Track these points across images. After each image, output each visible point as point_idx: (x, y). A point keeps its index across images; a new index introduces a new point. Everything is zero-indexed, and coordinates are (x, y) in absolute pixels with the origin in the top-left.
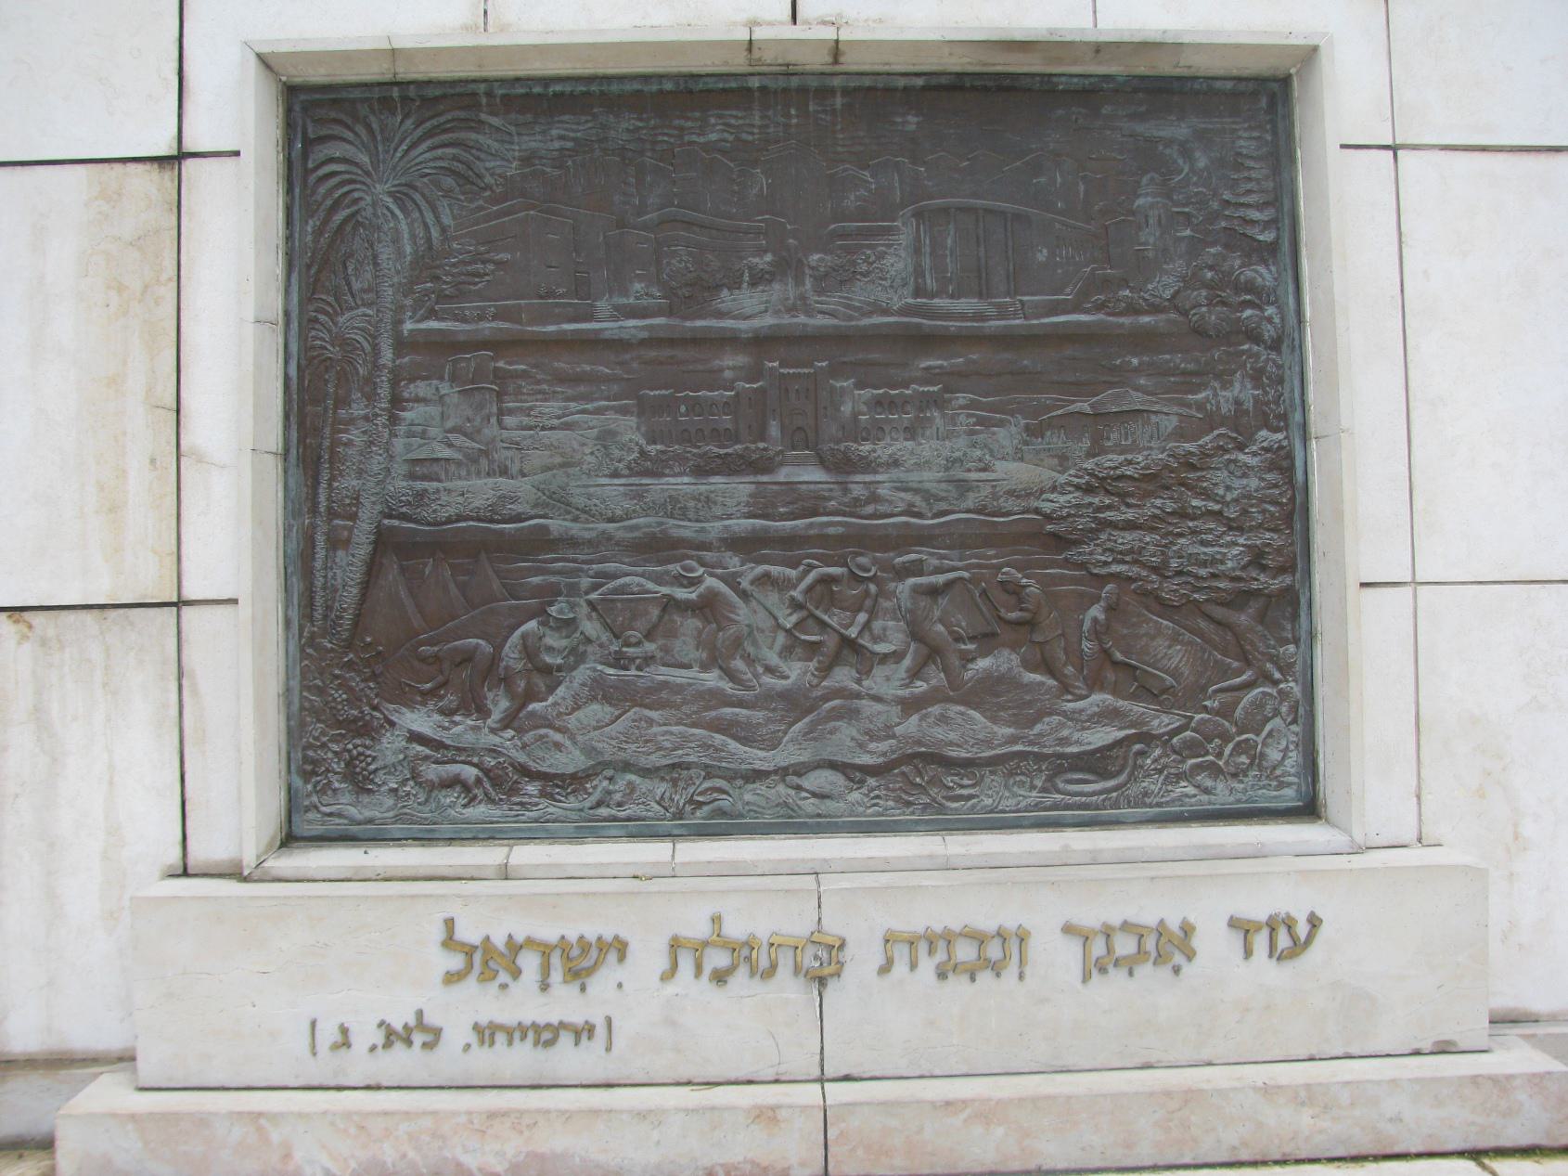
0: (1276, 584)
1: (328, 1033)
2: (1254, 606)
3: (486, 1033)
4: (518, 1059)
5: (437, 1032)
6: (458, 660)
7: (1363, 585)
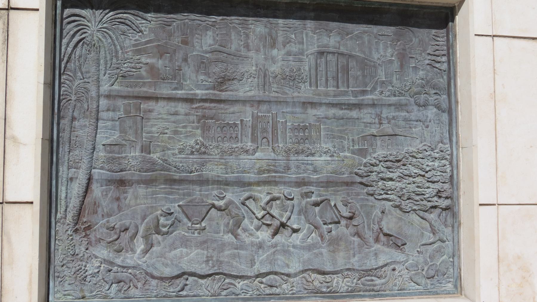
0: (447, 202)
2: (438, 211)
6: (123, 229)
7: (480, 205)
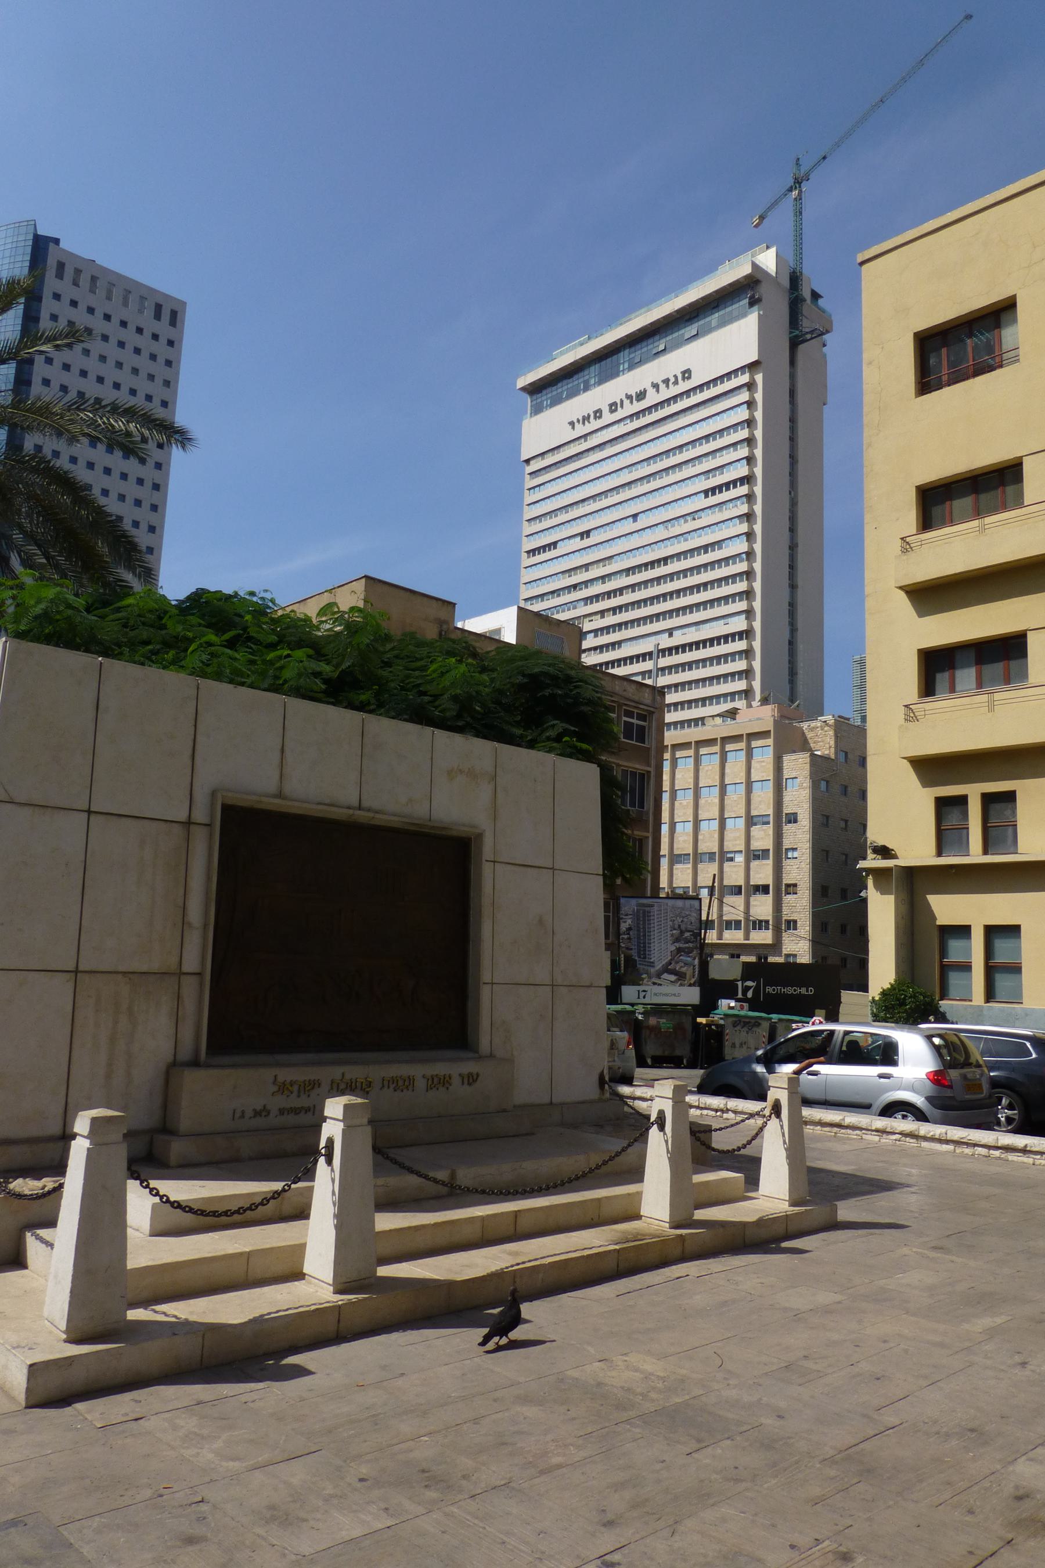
1: (237, 1115)
3: (282, 1111)
4: (290, 1119)
5: (269, 1113)
